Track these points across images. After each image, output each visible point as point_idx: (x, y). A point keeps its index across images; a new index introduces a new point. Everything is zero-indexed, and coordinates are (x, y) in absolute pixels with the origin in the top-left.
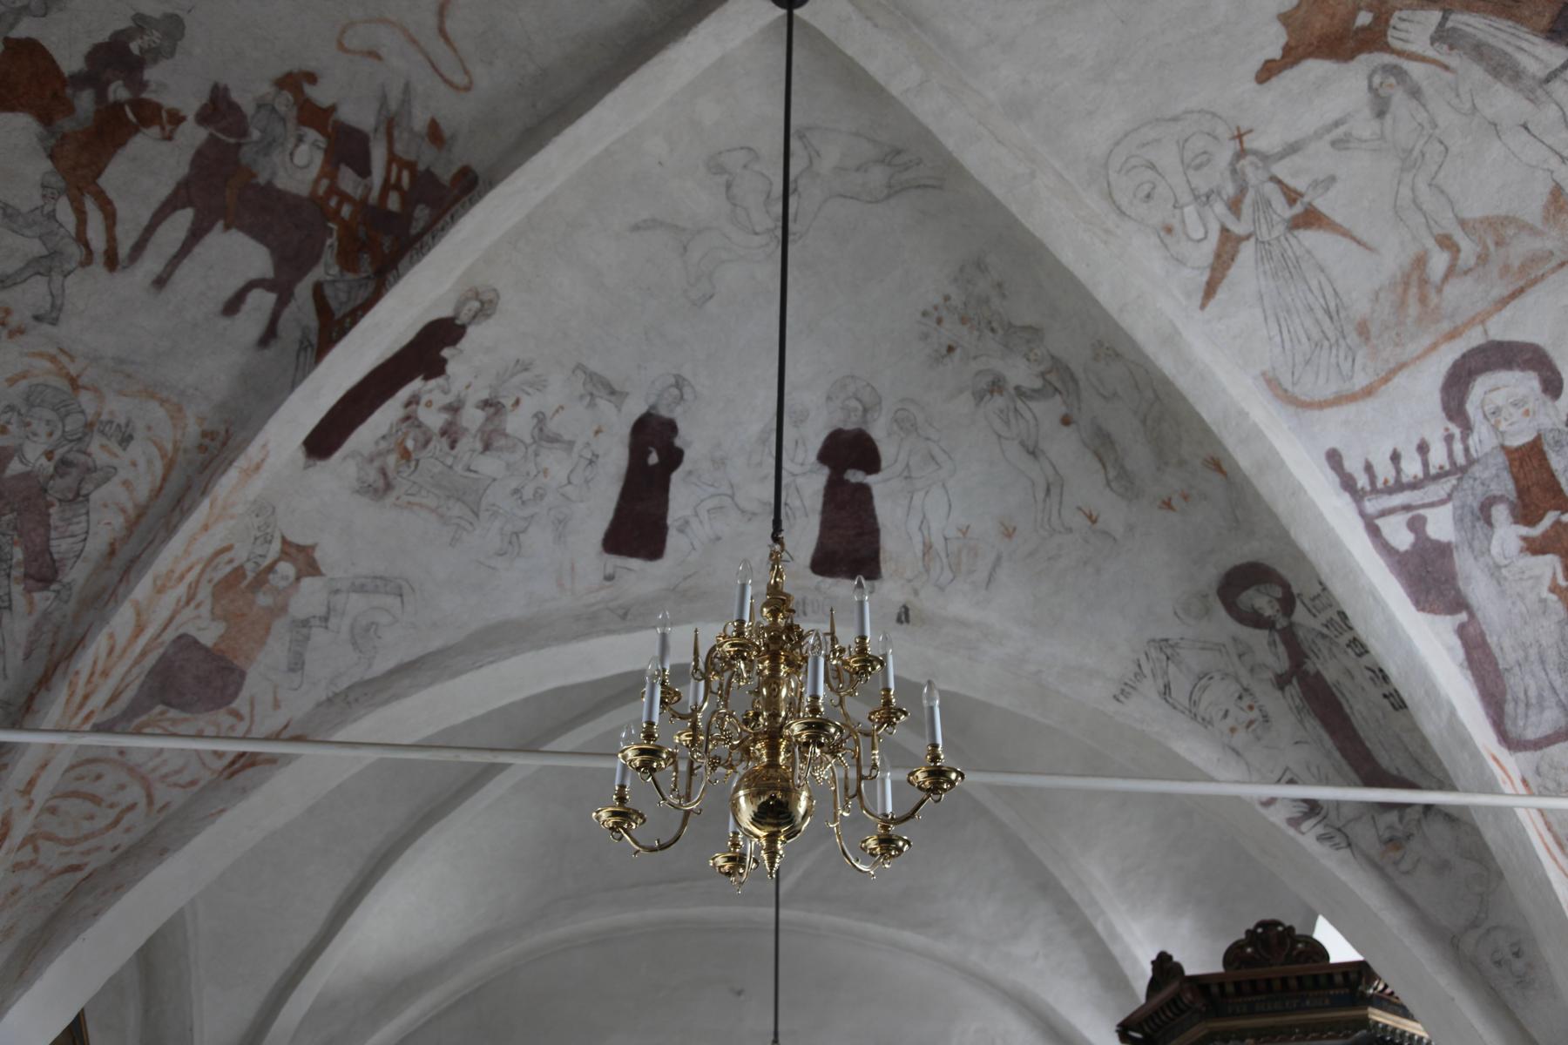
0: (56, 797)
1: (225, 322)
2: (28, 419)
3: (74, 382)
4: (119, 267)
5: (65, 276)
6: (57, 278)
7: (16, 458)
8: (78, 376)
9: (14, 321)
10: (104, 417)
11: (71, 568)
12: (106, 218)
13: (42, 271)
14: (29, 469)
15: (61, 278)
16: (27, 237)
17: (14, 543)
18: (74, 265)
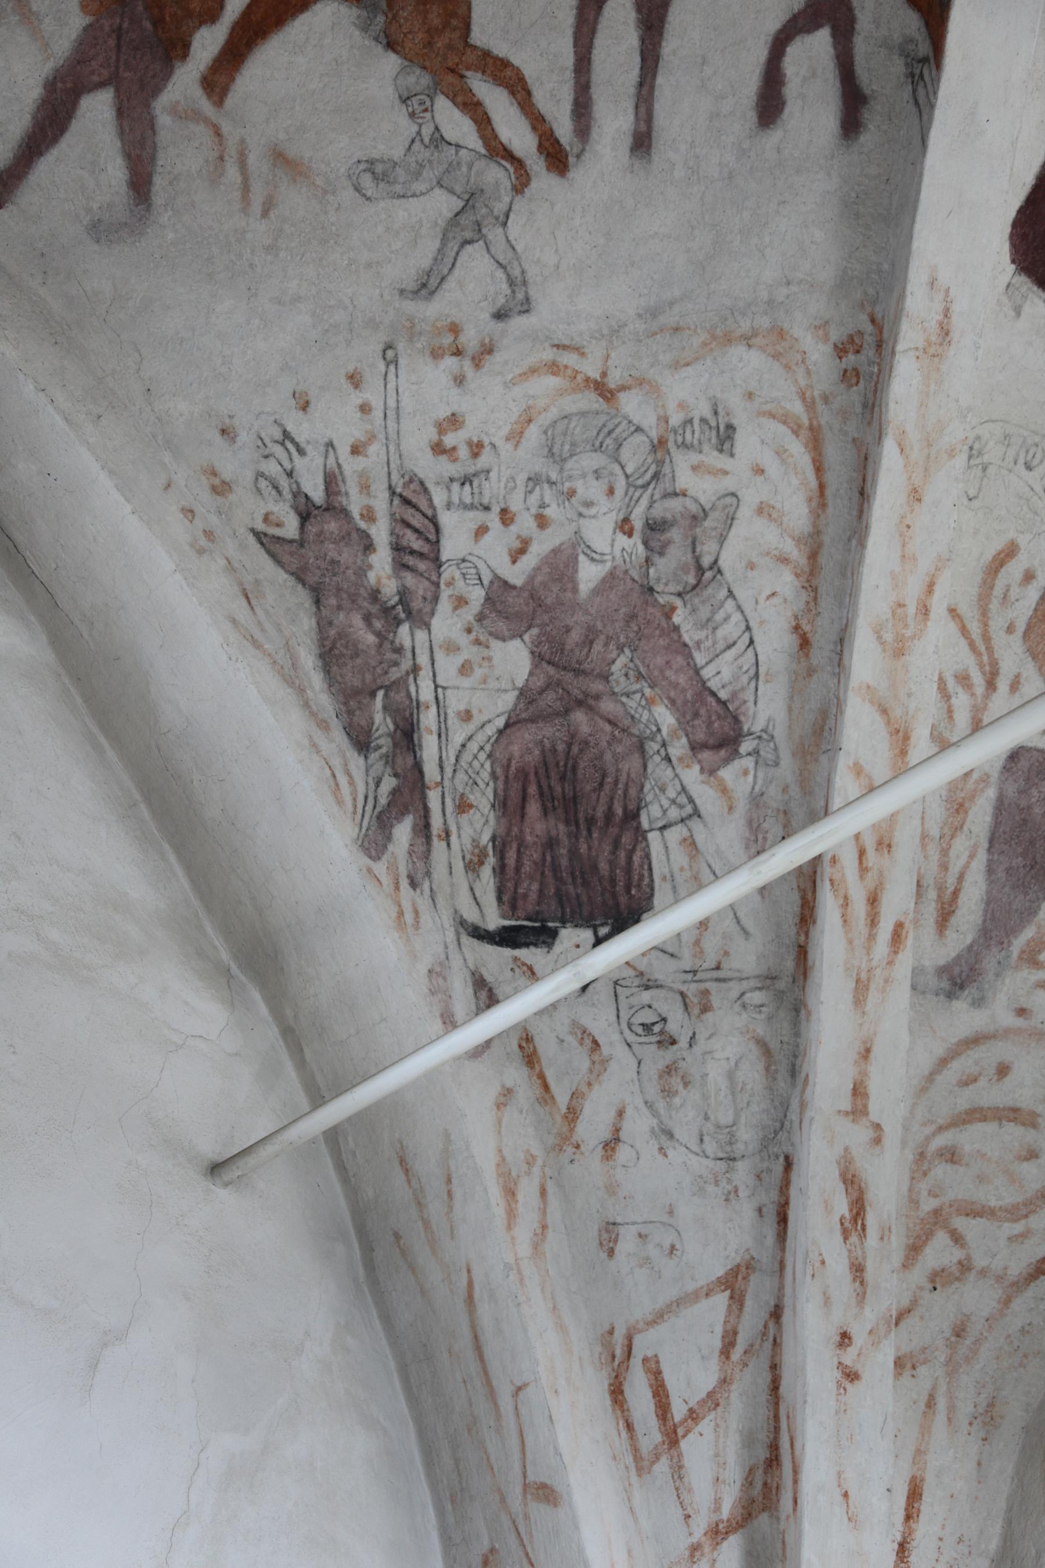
0: (941, 1129)
1: (774, 136)
2: (567, 485)
3: (602, 389)
4: (571, 160)
5: (505, 224)
6: (494, 234)
7: (582, 558)
8: (604, 374)
9: (470, 339)
10: (676, 419)
11: (755, 703)
12: (513, 93)
13: (468, 235)
14: (609, 565)
15: (500, 230)
16: (422, 194)
17: (651, 702)
18: (507, 199)
